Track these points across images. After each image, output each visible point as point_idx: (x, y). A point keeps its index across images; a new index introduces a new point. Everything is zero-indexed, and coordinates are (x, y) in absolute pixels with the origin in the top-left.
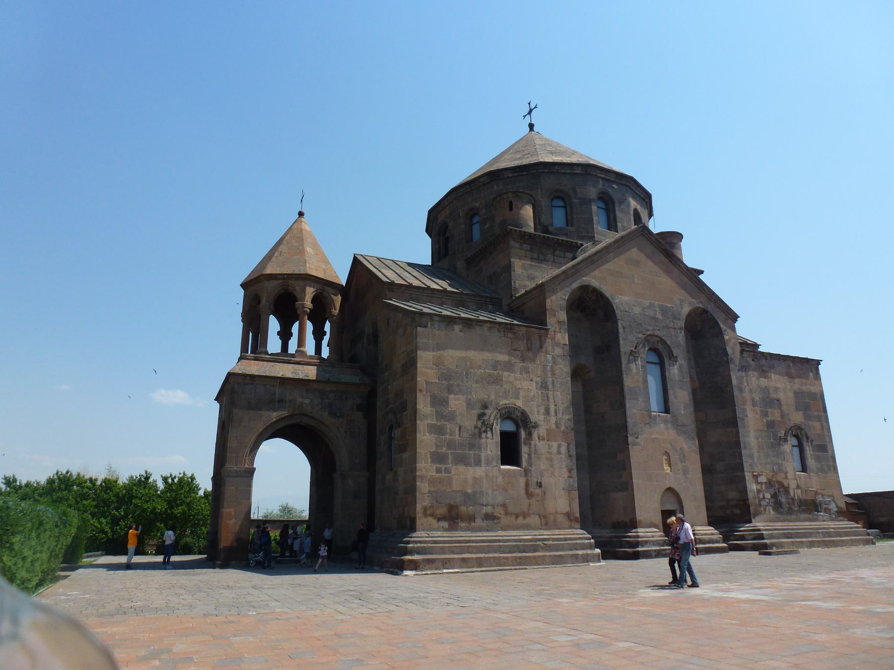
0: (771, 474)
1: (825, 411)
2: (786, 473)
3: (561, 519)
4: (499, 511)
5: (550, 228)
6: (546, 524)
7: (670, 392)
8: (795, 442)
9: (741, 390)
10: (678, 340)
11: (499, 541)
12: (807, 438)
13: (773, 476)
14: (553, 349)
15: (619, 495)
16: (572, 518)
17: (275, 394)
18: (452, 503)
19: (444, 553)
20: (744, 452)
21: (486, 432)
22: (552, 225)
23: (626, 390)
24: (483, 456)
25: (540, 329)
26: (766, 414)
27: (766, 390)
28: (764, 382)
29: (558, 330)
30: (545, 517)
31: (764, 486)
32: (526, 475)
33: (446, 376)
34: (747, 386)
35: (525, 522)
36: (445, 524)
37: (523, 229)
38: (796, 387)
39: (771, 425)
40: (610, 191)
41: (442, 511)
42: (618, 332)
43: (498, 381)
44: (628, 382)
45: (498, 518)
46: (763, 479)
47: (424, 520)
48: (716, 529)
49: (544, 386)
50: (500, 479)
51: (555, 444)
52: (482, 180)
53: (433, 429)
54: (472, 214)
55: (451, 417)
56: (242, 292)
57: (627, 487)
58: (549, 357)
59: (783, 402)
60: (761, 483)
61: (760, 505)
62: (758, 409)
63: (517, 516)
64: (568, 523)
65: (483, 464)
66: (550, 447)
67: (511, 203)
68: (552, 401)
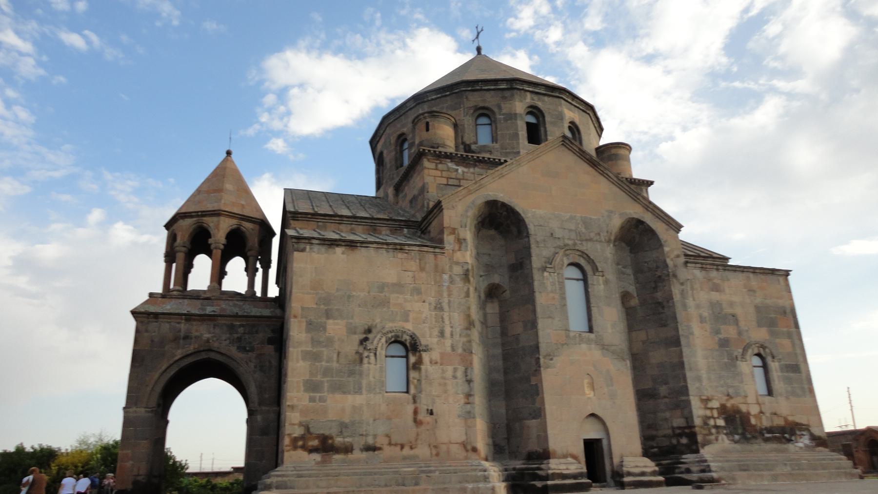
0: (726, 398)
1: (797, 326)
2: (746, 397)
3: (456, 450)
4: (381, 441)
5: (473, 147)
6: (437, 455)
7: (594, 311)
8: (757, 361)
9: (685, 306)
10: (605, 254)
11: (375, 474)
12: (773, 357)
13: (727, 400)
14: (451, 267)
15: (533, 423)
16: (469, 447)
17: (180, 331)
18: (327, 433)
19: (307, 487)
20: (689, 374)
21: (368, 357)
22: (476, 143)
23: (539, 310)
24: (364, 382)
25: (435, 247)
26: (718, 332)
27: (715, 306)
28: (715, 296)
29: (457, 247)
30: (435, 447)
31: (716, 414)
32: (415, 402)
33: (326, 300)
34: (694, 303)
35: (412, 452)
36: (317, 457)
37: (440, 149)
38: (758, 300)
39: (724, 343)
40: (540, 104)
41: (315, 443)
42: (528, 248)
43: (385, 303)
44: (541, 299)
45: (380, 449)
46: (715, 404)
47: (292, 453)
48: (653, 460)
49: (439, 307)
50: (383, 407)
51: (450, 369)
52: (408, 104)
53: (306, 356)
55: (330, 341)
56: (165, 233)
57: (539, 413)
58: (446, 277)
59: (741, 319)
60: (712, 409)
61: (711, 434)
62: (707, 326)
63: (402, 447)
64: (464, 454)
65: (364, 391)
66: (443, 371)
67: (427, 123)
68: (447, 322)
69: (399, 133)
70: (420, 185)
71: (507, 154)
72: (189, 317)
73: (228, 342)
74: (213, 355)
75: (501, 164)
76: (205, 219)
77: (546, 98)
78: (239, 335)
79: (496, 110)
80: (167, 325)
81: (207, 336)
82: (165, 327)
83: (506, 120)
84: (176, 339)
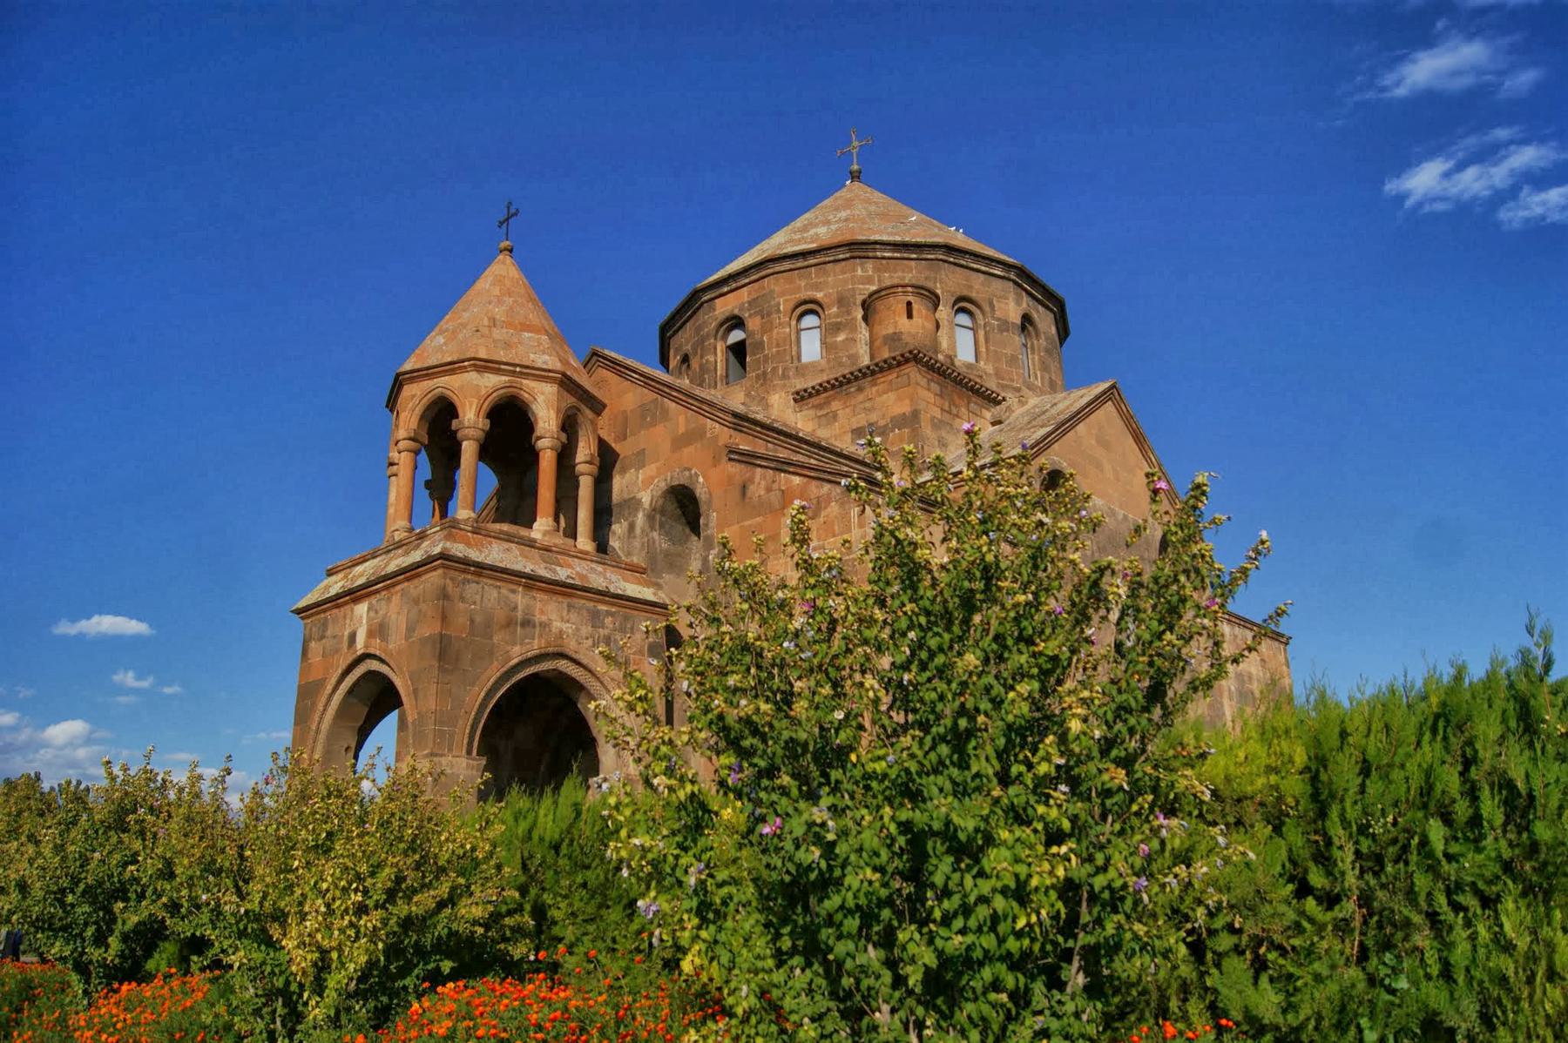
17: (515, 608)
40: (1035, 316)
54: (810, 307)
67: (909, 304)
69: (803, 295)
70: (904, 408)
71: (1003, 387)
72: (531, 582)
73: (590, 642)
74: (564, 666)
75: (999, 403)
76: (528, 383)
77: (1041, 308)
78: (606, 632)
79: (987, 309)
80: (495, 594)
81: (557, 624)
82: (488, 597)
83: (1001, 331)
84: (510, 623)
